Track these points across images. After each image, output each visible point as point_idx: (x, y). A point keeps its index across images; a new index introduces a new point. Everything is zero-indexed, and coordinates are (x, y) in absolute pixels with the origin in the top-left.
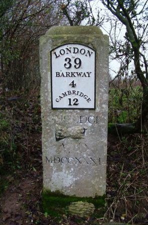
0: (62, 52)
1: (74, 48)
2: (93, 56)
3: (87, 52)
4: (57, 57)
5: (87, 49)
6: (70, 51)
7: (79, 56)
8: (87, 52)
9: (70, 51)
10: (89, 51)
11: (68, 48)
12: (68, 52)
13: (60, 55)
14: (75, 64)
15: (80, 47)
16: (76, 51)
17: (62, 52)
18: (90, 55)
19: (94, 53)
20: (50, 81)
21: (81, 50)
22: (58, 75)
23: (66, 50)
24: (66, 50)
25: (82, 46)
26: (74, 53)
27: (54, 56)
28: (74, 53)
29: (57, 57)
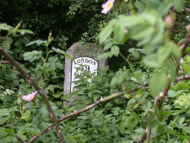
0: (79, 61)
1: (86, 60)
2: (97, 64)
3: (93, 62)
4: (75, 64)
5: (93, 60)
6: (83, 61)
7: (88, 64)
8: (93, 62)
9: (83, 61)
10: (94, 62)
11: (82, 59)
12: (82, 61)
13: (78, 63)
14: (86, 69)
15: (89, 59)
16: (87, 61)
17: (79, 61)
18: (95, 64)
19: (97, 63)
20: (70, 77)
21: (90, 61)
22: (75, 74)
23: (81, 60)
24: (81, 60)
25: (90, 58)
26: (86, 62)
27: (73, 63)
28: (86, 62)
29: (75, 64)
